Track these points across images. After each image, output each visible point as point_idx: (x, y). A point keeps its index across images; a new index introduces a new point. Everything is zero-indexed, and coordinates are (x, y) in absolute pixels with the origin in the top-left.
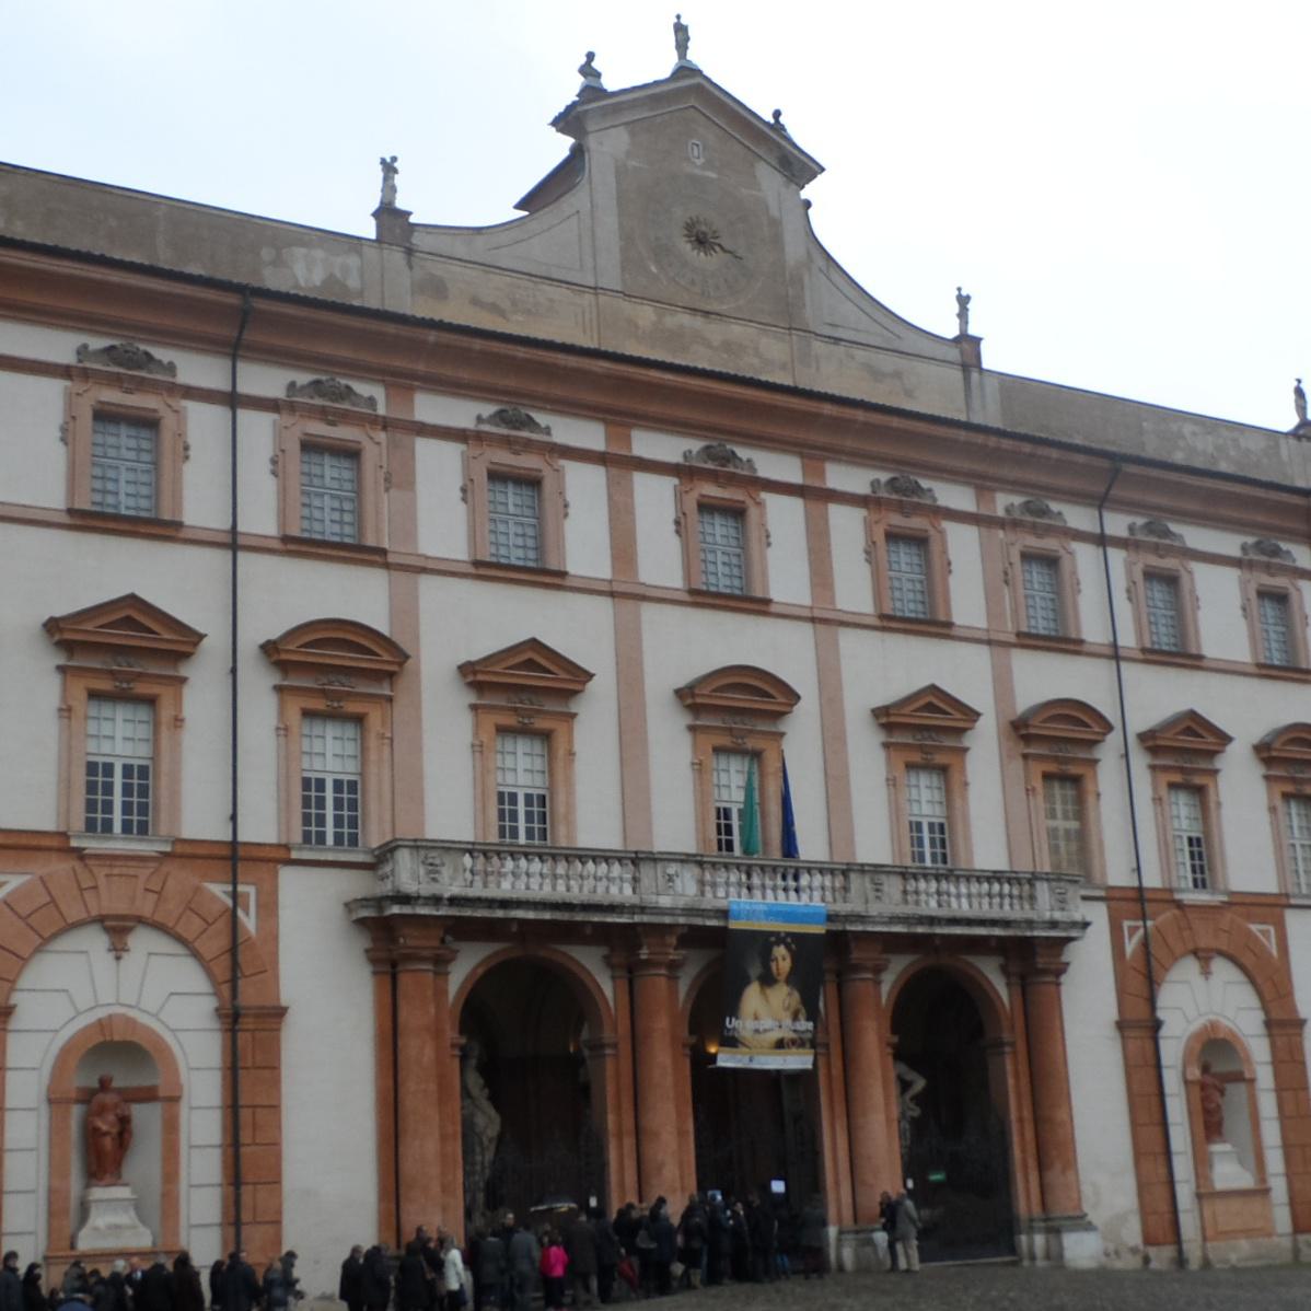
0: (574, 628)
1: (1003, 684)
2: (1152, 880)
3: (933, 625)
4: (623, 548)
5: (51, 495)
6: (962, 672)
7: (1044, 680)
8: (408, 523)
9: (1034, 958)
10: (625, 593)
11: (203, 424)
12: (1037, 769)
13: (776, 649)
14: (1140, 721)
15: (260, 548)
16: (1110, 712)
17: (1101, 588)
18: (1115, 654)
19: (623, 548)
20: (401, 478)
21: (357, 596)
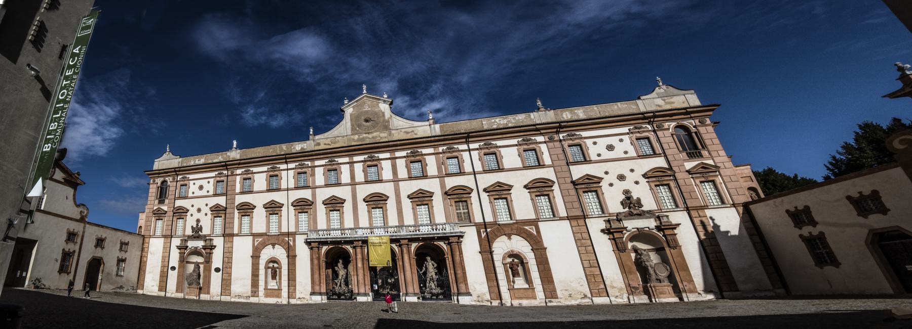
0: (342, 192)
1: (443, 185)
2: (489, 218)
3: (540, 165)
4: (353, 177)
5: (265, 188)
6: (431, 185)
7: (451, 182)
8: (314, 181)
9: (455, 240)
10: (353, 184)
11: (284, 173)
12: (453, 201)
13: (466, 181)
14: (482, 187)
15: (292, 189)
16: (473, 186)
17: (510, 155)
18: (474, 173)
19: (353, 177)
20: (313, 175)
21: (306, 194)
